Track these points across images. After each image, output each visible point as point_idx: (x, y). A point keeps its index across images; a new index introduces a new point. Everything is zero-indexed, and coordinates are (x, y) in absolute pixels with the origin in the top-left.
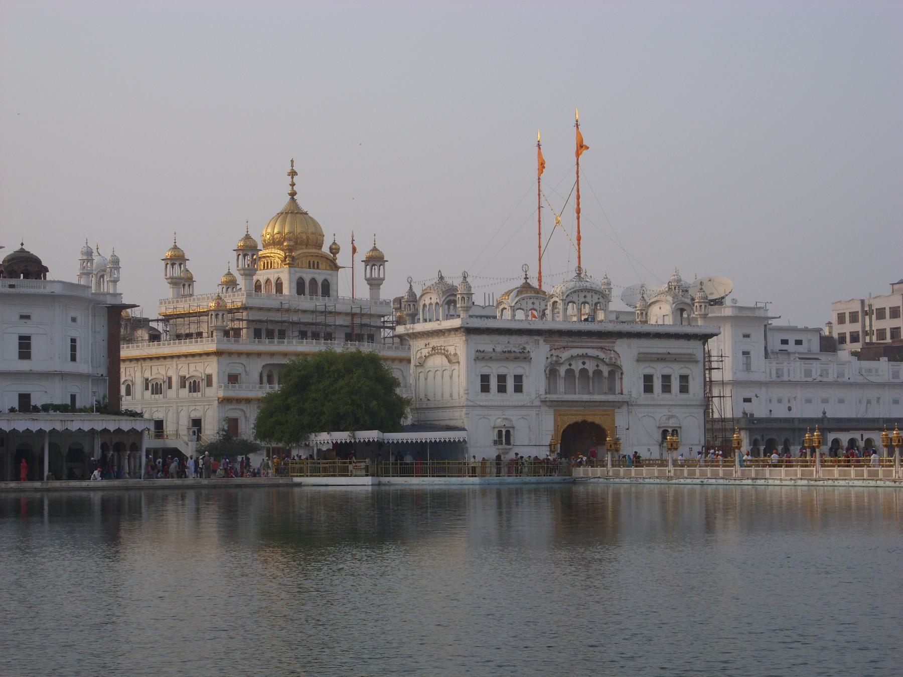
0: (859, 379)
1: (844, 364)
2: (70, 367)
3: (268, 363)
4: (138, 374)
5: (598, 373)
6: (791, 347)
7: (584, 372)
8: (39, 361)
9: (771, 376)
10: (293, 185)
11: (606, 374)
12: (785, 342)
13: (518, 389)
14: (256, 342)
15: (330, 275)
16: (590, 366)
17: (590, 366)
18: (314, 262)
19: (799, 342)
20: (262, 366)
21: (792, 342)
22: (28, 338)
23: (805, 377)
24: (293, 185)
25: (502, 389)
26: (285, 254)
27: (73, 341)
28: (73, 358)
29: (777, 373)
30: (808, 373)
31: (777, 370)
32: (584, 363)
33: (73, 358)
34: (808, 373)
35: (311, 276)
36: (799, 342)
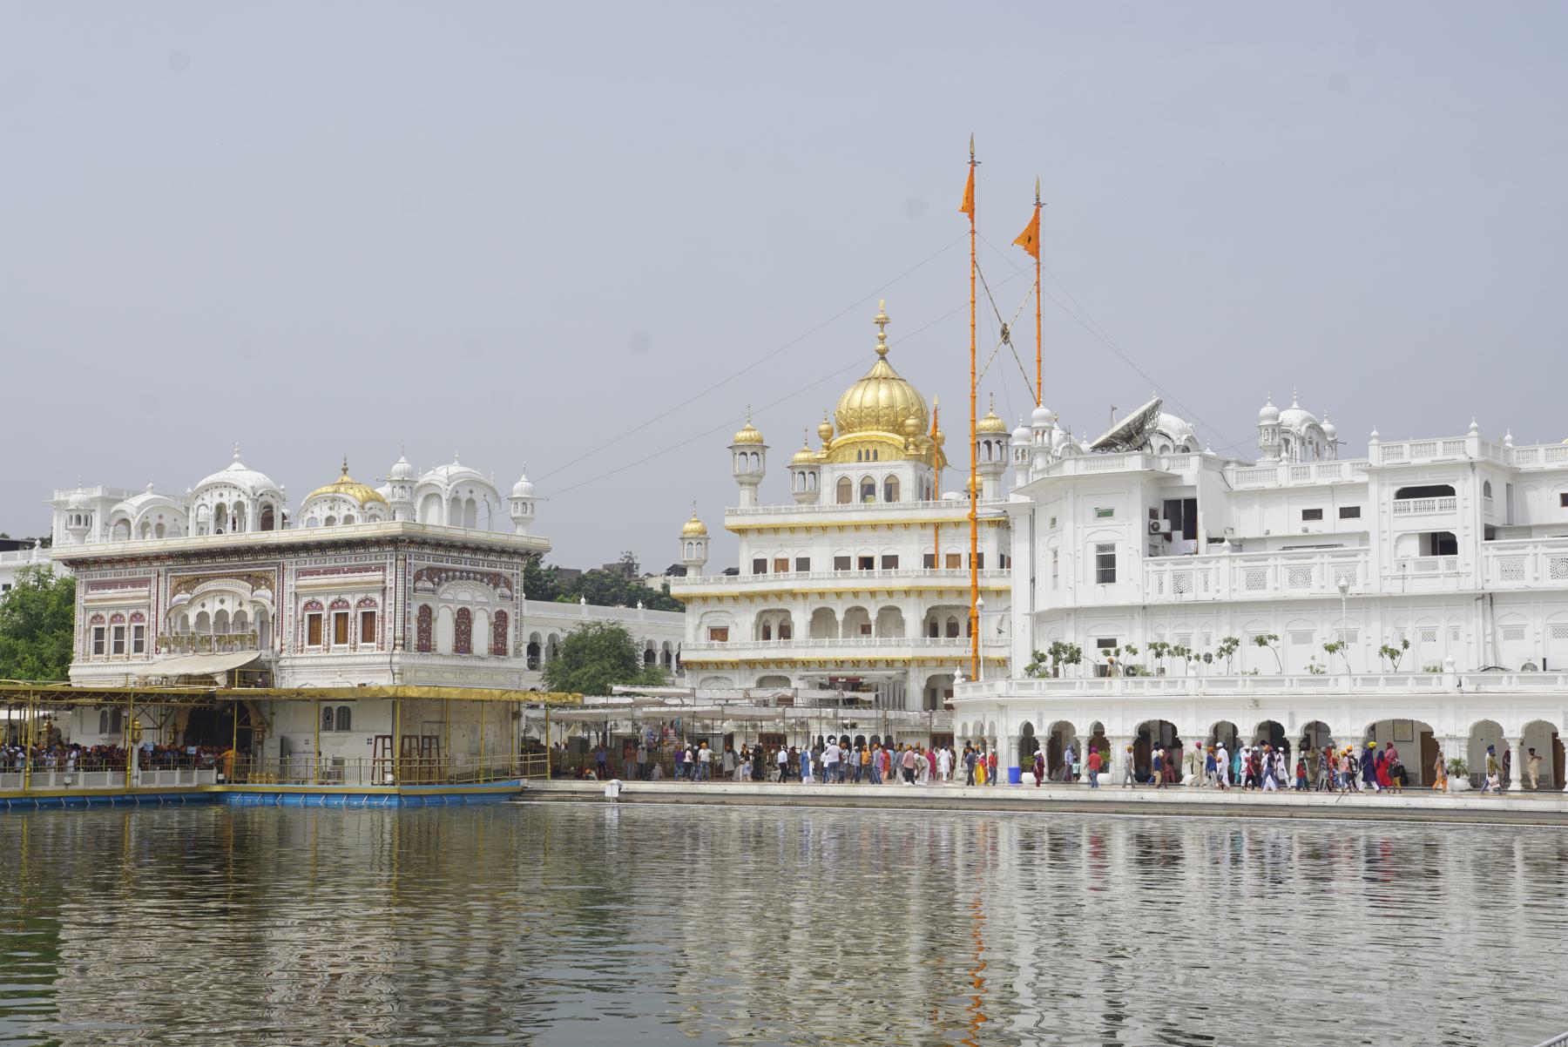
0: (1395, 588)
1: (1356, 556)
3: (764, 608)
6: (1331, 522)
7: (221, 614)
9: (1161, 591)
12: (1311, 515)
14: (928, 573)
15: (900, 466)
16: (230, 607)
17: (230, 607)
18: (868, 452)
20: (845, 609)
23: (1249, 587)
26: (906, 440)
29: (1177, 584)
31: (1178, 578)
32: (222, 602)
35: (863, 473)
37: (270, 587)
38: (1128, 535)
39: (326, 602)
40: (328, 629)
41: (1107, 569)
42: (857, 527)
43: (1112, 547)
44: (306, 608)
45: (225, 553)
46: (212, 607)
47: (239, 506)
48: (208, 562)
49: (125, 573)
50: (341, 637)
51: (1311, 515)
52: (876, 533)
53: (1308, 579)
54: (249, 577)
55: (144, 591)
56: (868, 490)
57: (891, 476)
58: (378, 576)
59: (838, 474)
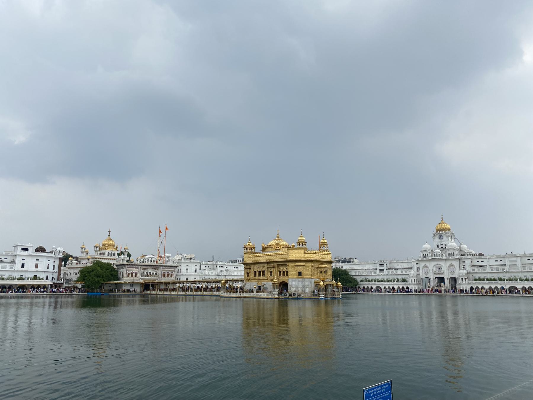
2: (48, 270)
4: (72, 271)
5: (153, 273)
8: (39, 269)
10: (109, 234)
11: (155, 273)
12: (206, 267)
13: (136, 276)
16: (151, 272)
17: (151, 272)
19: (209, 267)
21: (207, 267)
22: (38, 264)
24: (109, 234)
25: (132, 276)
27: (48, 265)
28: (48, 268)
30: (208, 273)
33: (48, 268)
34: (208, 273)
35: (111, 252)
36: (209, 267)
37: (158, 270)
38: (198, 268)
39: (166, 272)
40: (166, 275)
41: (196, 271)
42: (111, 259)
43: (196, 269)
44: (163, 273)
45: (152, 265)
46: (149, 272)
47: (154, 260)
48: (148, 266)
49: (134, 267)
50: (168, 276)
51: (206, 267)
52: (113, 260)
53: (212, 273)
54: (154, 269)
55: (138, 269)
56: (111, 253)
57: (114, 253)
58: (174, 270)
59: (108, 252)
